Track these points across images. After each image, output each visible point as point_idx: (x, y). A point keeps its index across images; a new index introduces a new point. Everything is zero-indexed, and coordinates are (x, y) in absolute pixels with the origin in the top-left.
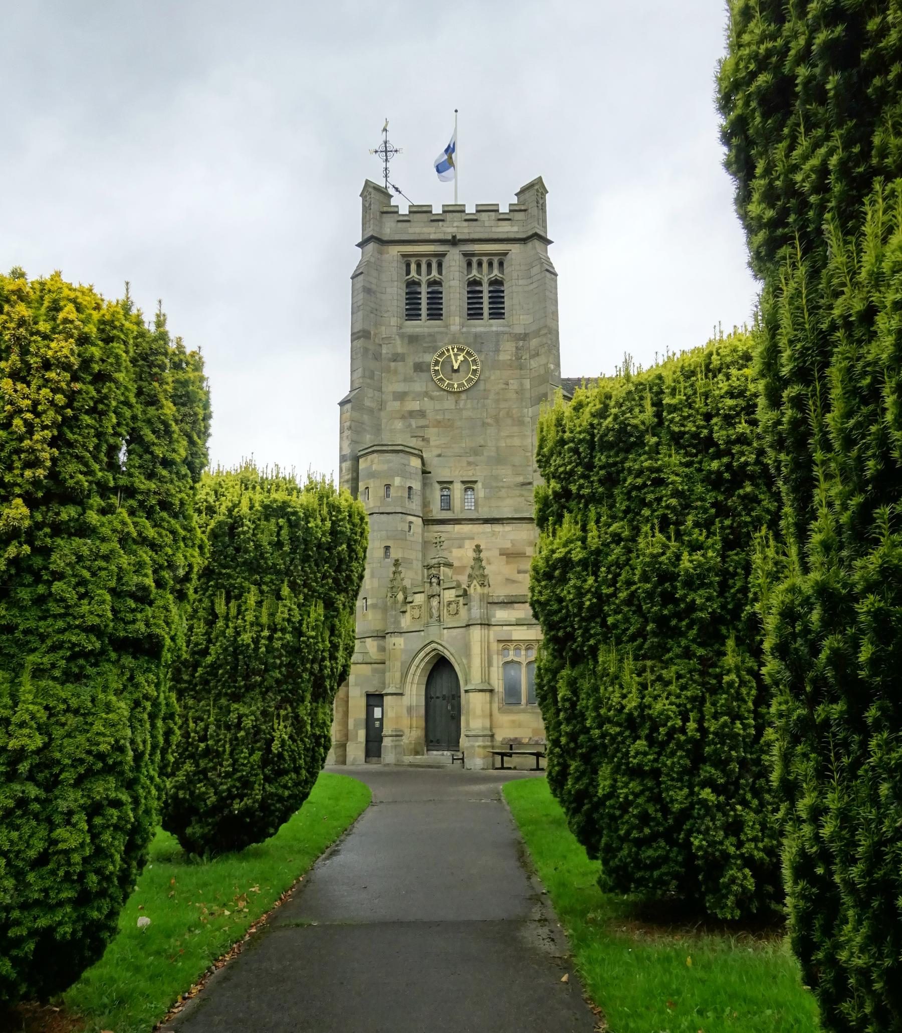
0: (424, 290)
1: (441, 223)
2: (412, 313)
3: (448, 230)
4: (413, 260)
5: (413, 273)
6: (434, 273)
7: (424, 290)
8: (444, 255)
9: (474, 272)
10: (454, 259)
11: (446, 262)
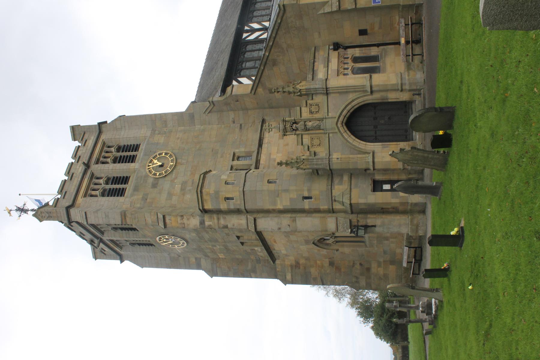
0: (109, 186)
1: (74, 175)
2: (121, 193)
3: (80, 168)
4: (89, 192)
5: (97, 193)
6: (101, 181)
7: (109, 186)
8: (92, 175)
9: (109, 160)
10: (96, 168)
11: (97, 174)
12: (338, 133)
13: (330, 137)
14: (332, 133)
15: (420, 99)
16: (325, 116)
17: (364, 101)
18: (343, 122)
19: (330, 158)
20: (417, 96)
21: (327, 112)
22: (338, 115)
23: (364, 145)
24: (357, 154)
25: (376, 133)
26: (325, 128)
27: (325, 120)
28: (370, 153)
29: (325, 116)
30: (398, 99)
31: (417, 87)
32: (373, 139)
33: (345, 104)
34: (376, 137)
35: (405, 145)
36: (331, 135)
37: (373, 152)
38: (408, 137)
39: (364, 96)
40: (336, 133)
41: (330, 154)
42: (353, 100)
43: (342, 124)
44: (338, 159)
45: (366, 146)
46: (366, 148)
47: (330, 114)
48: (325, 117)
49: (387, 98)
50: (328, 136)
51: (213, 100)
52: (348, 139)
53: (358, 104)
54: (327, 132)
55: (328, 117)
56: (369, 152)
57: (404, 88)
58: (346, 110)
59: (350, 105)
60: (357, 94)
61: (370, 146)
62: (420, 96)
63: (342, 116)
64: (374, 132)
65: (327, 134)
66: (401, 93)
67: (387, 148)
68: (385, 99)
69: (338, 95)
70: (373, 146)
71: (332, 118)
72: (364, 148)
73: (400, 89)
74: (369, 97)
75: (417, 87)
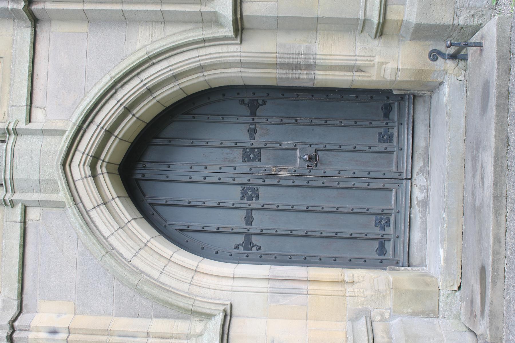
12: (67, 206)
13: (29, 224)
14: (40, 204)
15: (461, 78)
16: (17, 122)
17: (202, 68)
18: (96, 158)
19: (16, 324)
20: (450, 64)
21: (24, 102)
22: (74, 120)
23: (190, 275)
24: (150, 317)
25: (249, 220)
26: (8, 177)
27: (13, 137)
28: (209, 316)
29: (17, 122)
30: (360, 69)
31: (456, 16)
32: (237, 247)
33: (113, 74)
34: (248, 235)
35: (382, 287)
36: (33, 214)
37: (225, 311)
38: (389, 246)
39: (204, 41)
40: (59, 205)
41: (24, 302)
42: (150, 59)
43: (93, 167)
44: (54, 332)
45: (198, 278)
46: (194, 290)
47: (38, 114)
48: (11, 127)
49: (312, 61)
50: (19, 218)
51: (16, 128)
52: (113, 240)
53: (176, 77)
54: (16, 197)
55: (30, 126)
56: (207, 309)
57: (391, 16)
58: (112, 103)
59: (136, 81)
60: (171, 30)
61: (213, 282)
62: (462, 64)
63: (93, 127)
64: (243, 213)
65: (18, 209)
66: (376, 42)
67: (293, 298)
68: (297, 67)
69: (83, 28)
70: (227, 284)
71: (44, 132)
72: (185, 287)
73: (376, 21)
74: (225, 49)
75: (456, 16)
